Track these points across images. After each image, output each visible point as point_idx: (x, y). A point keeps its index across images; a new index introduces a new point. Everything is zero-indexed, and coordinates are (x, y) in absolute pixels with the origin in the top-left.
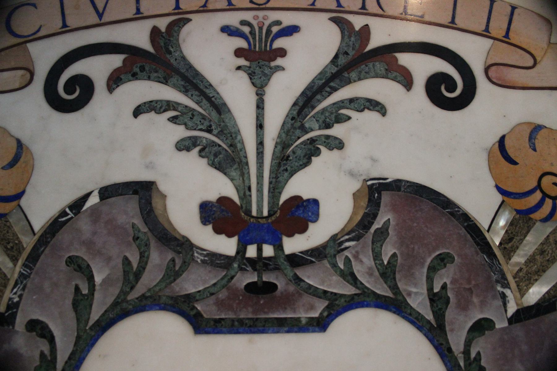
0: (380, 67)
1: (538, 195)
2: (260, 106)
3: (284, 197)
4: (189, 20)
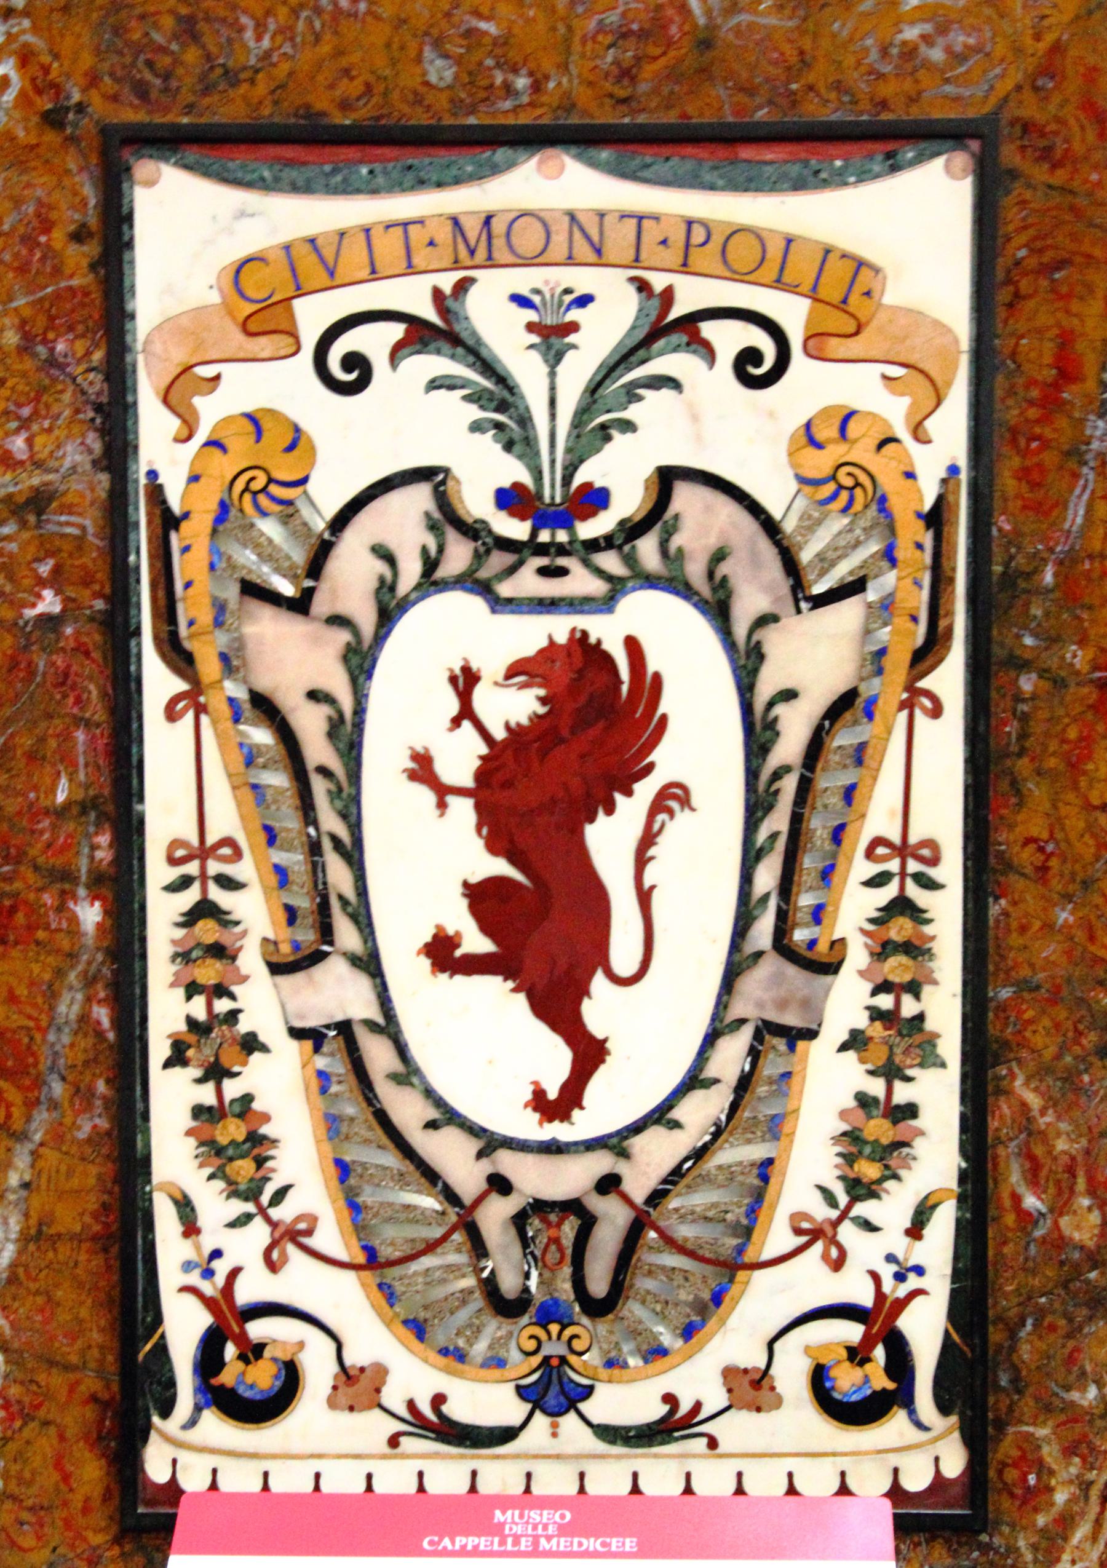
0: (681, 338)
2: (553, 388)
3: (579, 479)
4: (471, 281)
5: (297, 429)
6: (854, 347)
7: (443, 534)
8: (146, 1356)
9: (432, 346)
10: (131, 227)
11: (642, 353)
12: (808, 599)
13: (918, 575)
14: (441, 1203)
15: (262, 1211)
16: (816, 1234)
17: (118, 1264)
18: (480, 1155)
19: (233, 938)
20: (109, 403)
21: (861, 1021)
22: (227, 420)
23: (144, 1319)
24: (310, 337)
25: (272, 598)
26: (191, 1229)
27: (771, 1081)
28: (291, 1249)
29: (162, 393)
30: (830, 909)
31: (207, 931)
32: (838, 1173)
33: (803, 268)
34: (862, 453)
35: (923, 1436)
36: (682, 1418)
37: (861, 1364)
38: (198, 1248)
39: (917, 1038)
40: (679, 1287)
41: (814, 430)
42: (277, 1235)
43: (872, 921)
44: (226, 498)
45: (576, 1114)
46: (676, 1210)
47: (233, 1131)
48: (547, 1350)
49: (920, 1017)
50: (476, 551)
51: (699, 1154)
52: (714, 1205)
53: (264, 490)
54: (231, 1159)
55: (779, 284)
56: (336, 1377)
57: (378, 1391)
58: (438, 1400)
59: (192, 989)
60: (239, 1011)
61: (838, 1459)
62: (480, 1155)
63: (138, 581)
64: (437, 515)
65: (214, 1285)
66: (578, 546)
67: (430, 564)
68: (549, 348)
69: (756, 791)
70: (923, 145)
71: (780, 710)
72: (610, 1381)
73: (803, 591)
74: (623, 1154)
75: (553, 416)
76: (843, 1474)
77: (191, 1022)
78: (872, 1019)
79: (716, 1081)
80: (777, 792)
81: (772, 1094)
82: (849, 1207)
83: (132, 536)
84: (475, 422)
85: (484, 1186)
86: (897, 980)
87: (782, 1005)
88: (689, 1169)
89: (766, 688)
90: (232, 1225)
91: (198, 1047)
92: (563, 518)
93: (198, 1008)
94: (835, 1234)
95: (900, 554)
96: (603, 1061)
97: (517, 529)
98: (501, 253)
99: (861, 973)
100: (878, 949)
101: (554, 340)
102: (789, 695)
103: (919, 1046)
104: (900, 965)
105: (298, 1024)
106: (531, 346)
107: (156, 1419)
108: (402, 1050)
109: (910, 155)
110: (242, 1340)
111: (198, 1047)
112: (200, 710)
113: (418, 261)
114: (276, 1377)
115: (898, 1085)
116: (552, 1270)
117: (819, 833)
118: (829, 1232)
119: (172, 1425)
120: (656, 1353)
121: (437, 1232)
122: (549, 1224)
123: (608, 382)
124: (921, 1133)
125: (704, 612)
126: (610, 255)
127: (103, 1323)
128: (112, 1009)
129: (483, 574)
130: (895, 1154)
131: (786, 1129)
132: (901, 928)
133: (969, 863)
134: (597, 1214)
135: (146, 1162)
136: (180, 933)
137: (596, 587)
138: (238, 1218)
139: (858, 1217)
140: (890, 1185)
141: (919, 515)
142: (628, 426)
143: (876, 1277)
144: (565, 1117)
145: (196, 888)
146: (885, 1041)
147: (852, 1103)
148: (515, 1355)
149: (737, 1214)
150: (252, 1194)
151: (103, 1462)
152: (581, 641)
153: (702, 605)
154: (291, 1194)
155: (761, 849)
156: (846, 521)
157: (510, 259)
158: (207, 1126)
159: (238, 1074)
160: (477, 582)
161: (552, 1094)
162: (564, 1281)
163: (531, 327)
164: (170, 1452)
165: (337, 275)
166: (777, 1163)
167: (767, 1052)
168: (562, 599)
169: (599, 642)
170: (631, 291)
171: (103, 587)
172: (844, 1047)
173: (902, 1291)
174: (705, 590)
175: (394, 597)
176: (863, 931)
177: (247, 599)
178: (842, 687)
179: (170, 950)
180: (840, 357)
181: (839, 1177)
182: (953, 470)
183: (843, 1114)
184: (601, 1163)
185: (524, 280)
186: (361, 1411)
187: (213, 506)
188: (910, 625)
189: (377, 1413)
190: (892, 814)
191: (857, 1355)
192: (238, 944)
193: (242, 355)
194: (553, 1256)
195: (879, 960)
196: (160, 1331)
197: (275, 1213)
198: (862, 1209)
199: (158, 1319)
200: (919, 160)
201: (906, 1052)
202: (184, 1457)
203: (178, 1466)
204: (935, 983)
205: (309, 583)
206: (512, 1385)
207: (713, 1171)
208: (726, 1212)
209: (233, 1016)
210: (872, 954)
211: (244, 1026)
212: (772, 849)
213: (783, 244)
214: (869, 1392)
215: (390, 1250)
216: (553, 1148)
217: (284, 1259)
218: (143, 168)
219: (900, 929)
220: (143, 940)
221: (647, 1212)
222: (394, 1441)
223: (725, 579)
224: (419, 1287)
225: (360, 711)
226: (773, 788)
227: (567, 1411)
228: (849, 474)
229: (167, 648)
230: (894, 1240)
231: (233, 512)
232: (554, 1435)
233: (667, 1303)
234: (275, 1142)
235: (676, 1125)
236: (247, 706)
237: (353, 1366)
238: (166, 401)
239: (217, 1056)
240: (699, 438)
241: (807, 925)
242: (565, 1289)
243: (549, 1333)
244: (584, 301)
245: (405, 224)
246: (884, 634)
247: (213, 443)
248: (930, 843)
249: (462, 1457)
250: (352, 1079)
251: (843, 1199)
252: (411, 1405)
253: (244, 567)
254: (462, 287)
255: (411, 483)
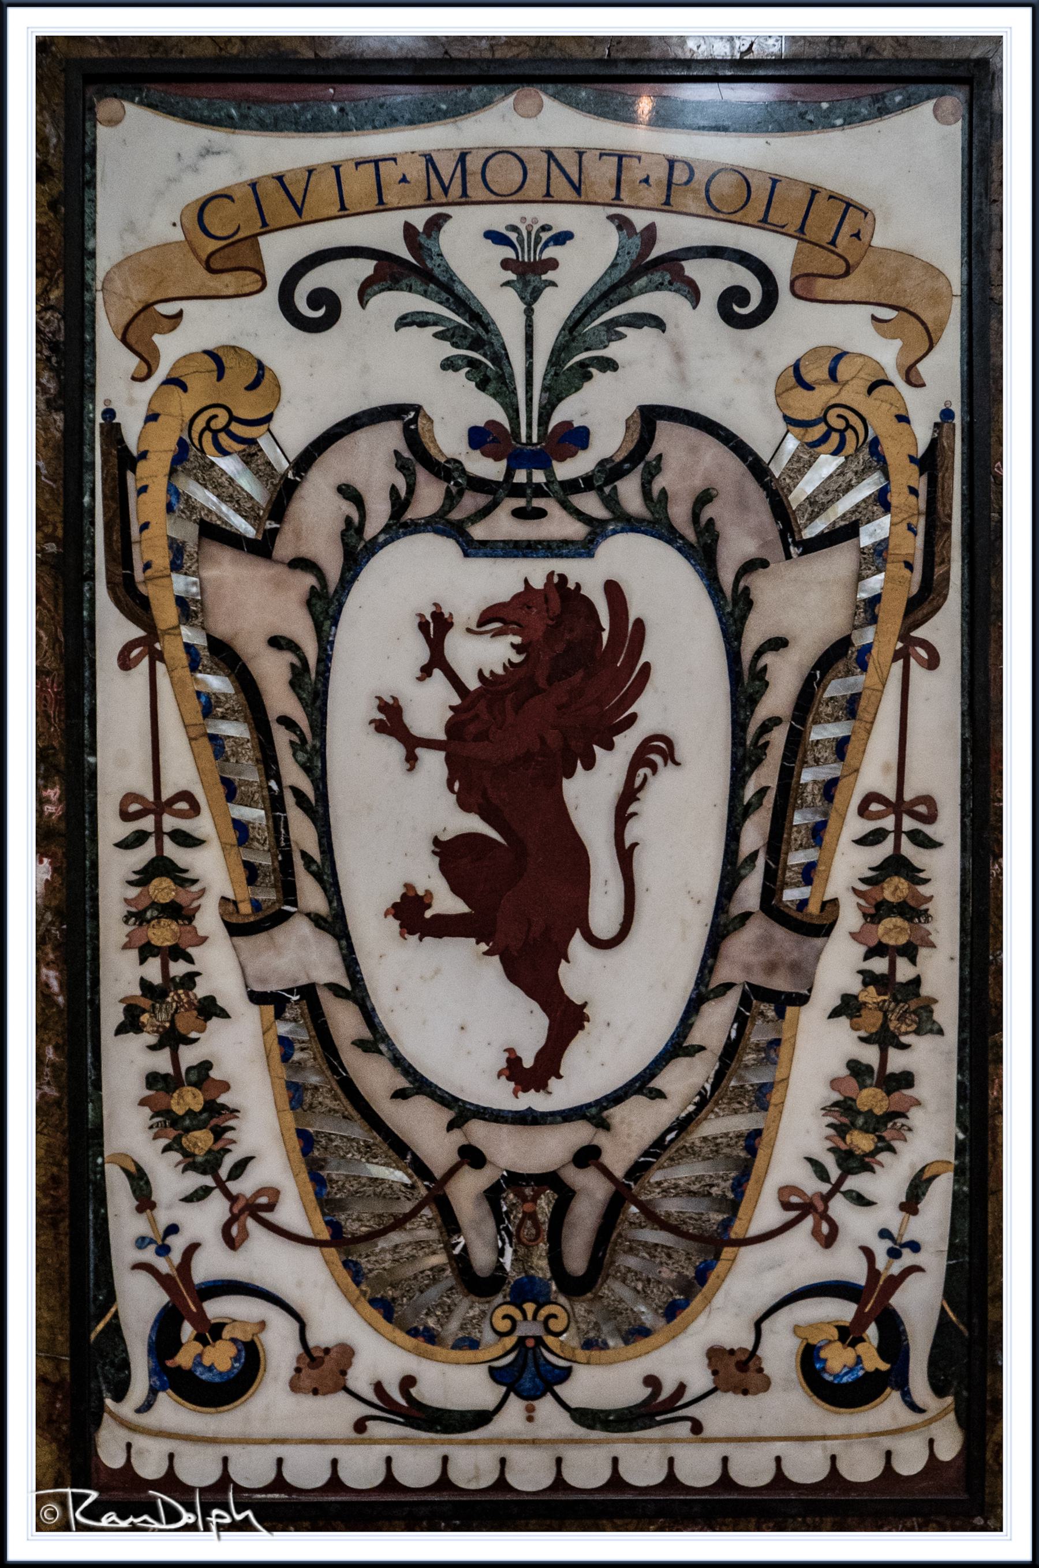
1: (820, 430)
2: (529, 326)
4: (447, 217)
5: (261, 366)
6: (845, 288)
7: (414, 474)
8: (97, 1337)
9: (405, 282)
10: (93, 165)
11: (623, 290)
12: (796, 544)
13: (913, 521)
14: (410, 1177)
15: (221, 1185)
16: (806, 1208)
17: (67, 1240)
18: (451, 1126)
19: (190, 897)
20: (64, 343)
21: (854, 985)
22: (188, 357)
23: (96, 1298)
24: (275, 273)
25: (232, 540)
26: (145, 1202)
27: (758, 1049)
28: (251, 1224)
29: (121, 331)
30: (821, 868)
31: (163, 889)
32: (829, 1144)
33: (787, 213)
34: (853, 395)
35: (917, 1418)
36: (665, 1401)
37: (853, 1344)
38: (153, 1222)
39: (913, 1004)
40: (661, 1263)
41: (803, 371)
42: (236, 1211)
43: (864, 880)
44: (186, 437)
45: (553, 1083)
46: (659, 1184)
47: (189, 1100)
48: (523, 1330)
49: (917, 982)
50: (448, 491)
51: (683, 1125)
52: (699, 1179)
53: (226, 429)
54: (187, 1130)
55: (764, 223)
56: (299, 1359)
57: (344, 1373)
58: (408, 1382)
59: (146, 951)
60: (198, 974)
61: (828, 1443)
62: (451, 1126)
63: (93, 524)
64: (407, 454)
65: (170, 1261)
66: (557, 487)
67: (399, 504)
68: (526, 284)
69: (744, 744)
70: (912, 88)
71: (768, 659)
72: (588, 1363)
73: (793, 536)
74: (603, 1125)
75: (530, 353)
76: (833, 1458)
77: (145, 985)
78: (865, 984)
79: (701, 1048)
80: (767, 744)
81: (760, 1062)
82: (841, 1180)
83: (87, 477)
84: (447, 359)
85: (455, 1158)
86: (892, 943)
87: (771, 968)
88: (672, 1141)
89: (753, 637)
90: (188, 1199)
91: (153, 1012)
92: (541, 459)
93: (153, 971)
94: (826, 1208)
95: (894, 499)
96: (582, 1027)
97: (490, 469)
98: (477, 191)
99: (854, 936)
100: (872, 911)
101: (531, 277)
102: (778, 644)
103: (914, 1012)
104: (895, 927)
105: (258, 988)
106: (507, 284)
107: (109, 1402)
108: (369, 1016)
109: (898, 99)
110: (200, 1319)
111: (153, 1012)
112: (156, 657)
113: (389, 198)
114: (236, 1359)
115: (893, 1053)
116: (527, 1247)
117: (809, 788)
118: (820, 1206)
119: (127, 1409)
120: (637, 1333)
121: (407, 1207)
122: (524, 1199)
123: (587, 320)
124: (918, 1103)
125: (687, 557)
126: (588, 194)
127: (52, 1302)
128: (61, 972)
129: (456, 515)
130: (890, 1125)
131: (775, 1098)
132: (897, 888)
133: (967, 821)
134: (576, 1189)
135: (97, 1133)
136: (133, 892)
137: (575, 530)
138: (196, 1191)
139: (851, 1191)
140: (883, 1157)
141: (912, 459)
142: (609, 365)
143: (868, 1253)
144: (541, 1085)
145: (150, 845)
146: (880, 1007)
147: (844, 1072)
148: (488, 1336)
149: (722, 1188)
150: (209, 1165)
151: (54, 1446)
152: (559, 584)
153: (686, 550)
154: (251, 1166)
155: (749, 804)
156: (840, 460)
157: (485, 195)
158: (162, 1094)
159: (195, 1040)
160: (450, 522)
161: (528, 1062)
162: (540, 1257)
163: (506, 264)
164: (124, 1435)
165: (304, 213)
166: (765, 1134)
167: (754, 1019)
168: (540, 542)
169: (578, 586)
170: (612, 228)
171: (55, 528)
172: (835, 1014)
173: (896, 1269)
174: (690, 535)
175: (361, 538)
176: (855, 890)
177: (206, 541)
178: (835, 637)
179: (121, 910)
180: (828, 298)
181: (830, 1150)
182: (947, 414)
183: (835, 1083)
184: (580, 1134)
185: (500, 217)
186: (325, 1394)
187: (171, 445)
188: (906, 572)
189: (342, 1396)
190: (886, 768)
191: (849, 1335)
192: (195, 904)
193: (201, 293)
194: (528, 1230)
195: (872, 922)
196: (113, 1310)
197: (234, 1187)
198: (854, 1183)
199: (111, 1297)
200: (908, 104)
201: (901, 1019)
202: (140, 1442)
203: (133, 1451)
204: (933, 946)
205: (270, 525)
206: (485, 1367)
207: (698, 1143)
208: (712, 1186)
209: (190, 980)
210: (865, 915)
211: (201, 991)
212: (760, 804)
213: (770, 184)
214: (861, 1373)
215: (356, 1225)
216: (529, 1119)
217: (245, 1234)
218: (106, 108)
219: (895, 889)
220: (95, 899)
221: (629, 1186)
222: (360, 1426)
223: (711, 521)
224: (387, 1265)
225: (325, 658)
226: (761, 742)
227: (542, 1395)
228: (839, 416)
229: (121, 591)
230: (889, 1216)
231: (193, 451)
232: (530, 1419)
233: (649, 1280)
234: (234, 1112)
235: (659, 1094)
236: (205, 653)
237: (317, 1347)
238: (124, 340)
239: (172, 1022)
240: (683, 378)
241: (797, 885)
242: (541, 1267)
243: (524, 1313)
244: (563, 238)
245: (376, 162)
246: (875, 583)
247: (174, 381)
248: (928, 800)
249: (433, 1442)
250: (317, 1047)
251: (834, 1173)
252: (379, 1388)
253: (203, 507)
254: (435, 224)
255: (379, 422)
